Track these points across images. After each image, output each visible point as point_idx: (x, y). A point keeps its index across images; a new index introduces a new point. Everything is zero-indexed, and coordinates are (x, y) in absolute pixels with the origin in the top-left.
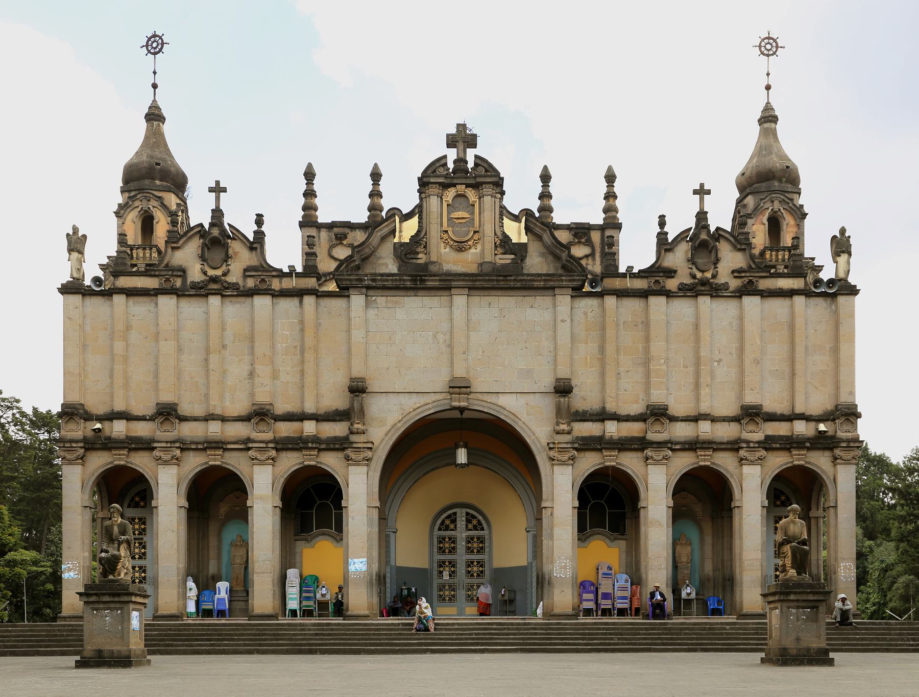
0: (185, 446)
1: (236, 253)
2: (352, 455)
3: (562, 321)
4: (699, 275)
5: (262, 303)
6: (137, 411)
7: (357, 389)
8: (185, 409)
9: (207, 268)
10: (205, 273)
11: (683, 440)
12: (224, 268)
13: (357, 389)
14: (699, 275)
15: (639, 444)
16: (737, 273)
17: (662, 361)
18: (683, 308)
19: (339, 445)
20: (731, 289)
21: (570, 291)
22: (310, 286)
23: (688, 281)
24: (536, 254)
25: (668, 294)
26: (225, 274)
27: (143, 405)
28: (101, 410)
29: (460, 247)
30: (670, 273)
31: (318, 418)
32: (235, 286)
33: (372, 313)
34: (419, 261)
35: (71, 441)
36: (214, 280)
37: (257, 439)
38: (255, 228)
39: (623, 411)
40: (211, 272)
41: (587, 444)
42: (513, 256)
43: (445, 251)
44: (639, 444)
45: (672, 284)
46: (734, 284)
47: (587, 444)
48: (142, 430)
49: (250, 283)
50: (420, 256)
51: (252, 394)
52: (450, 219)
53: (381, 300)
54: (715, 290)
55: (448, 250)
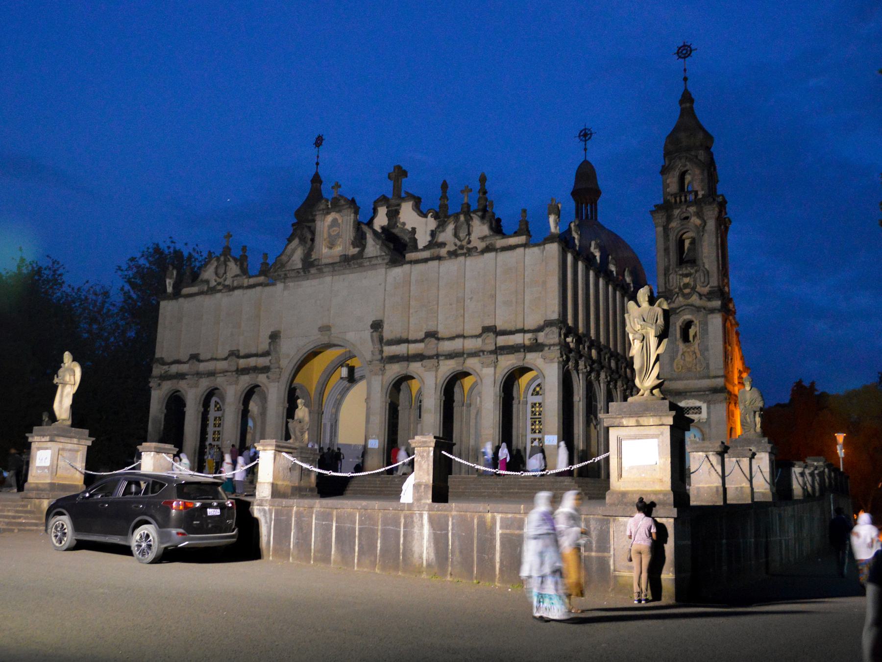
0: (199, 375)
4: (459, 243)
7: (274, 337)
9: (217, 279)
10: (216, 281)
11: (447, 353)
14: (459, 243)
15: (419, 357)
16: (483, 239)
17: (435, 303)
18: (450, 267)
19: (265, 369)
20: (479, 250)
22: (261, 281)
23: (453, 248)
25: (439, 258)
26: (225, 280)
27: (184, 355)
29: (331, 246)
30: (443, 245)
31: (256, 355)
33: (286, 293)
38: (241, 253)
40: (219, 280)
41: (394, 359)
43: (325, 250)
44: (419, 357)
45: (443, 252)
46: (481, 245)
47: (394, 359)
48: (184, 368)
52: (329, 233)
53: (291, 284)
54: (470, 252)
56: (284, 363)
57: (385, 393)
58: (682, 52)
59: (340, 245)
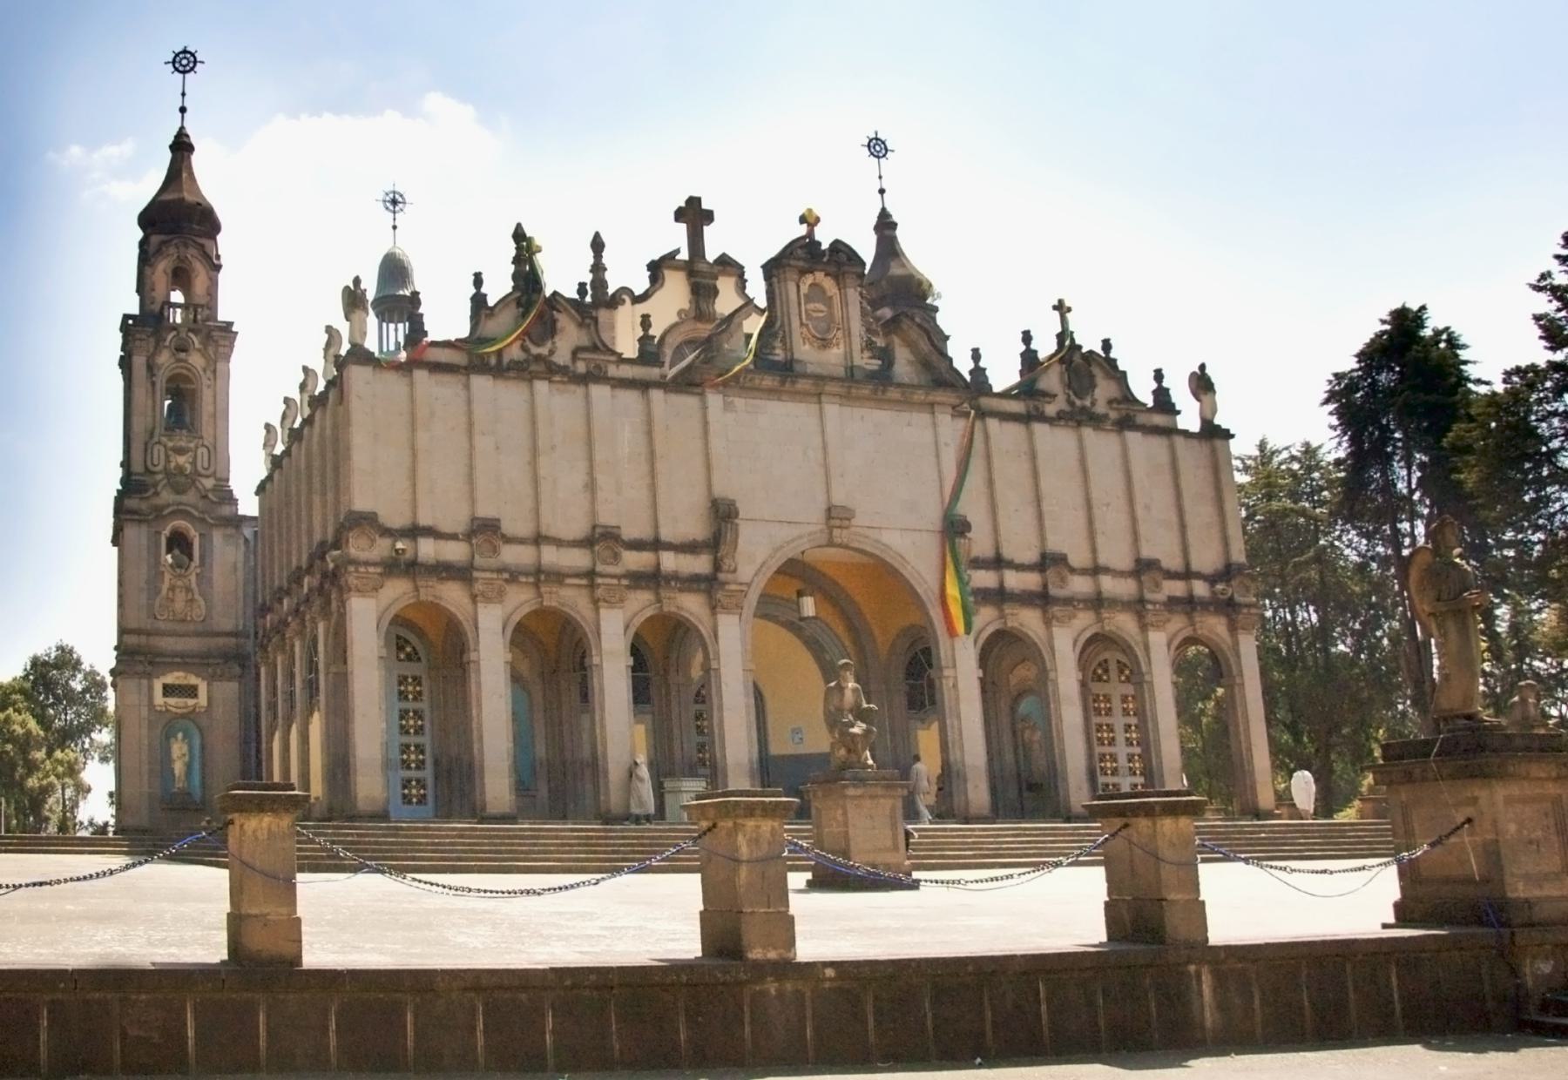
1: (563, 330)
2: (725, 601)
3: (946, 444)
5: (599, 392)
6: (446, 527)
7: (723, 514)
8: (508, 527)
12: (549, 345)
13: (723, 514)
21: (950, 410)
24: (904, 361)
28: (397, 521)
32: (563, 370)
34: (776, 358)
35: (367, 564)
36: (538, 358)
37: (604, 572)
39: (1018, 560)
40: (535, 350)
42: (880, 362)
49: (581, 367)
50: (778, 351)
51: (593, 513)
55: (807, 347)
56: (746, 571)
57: (1077, 656)
58: (189, 62)
59: (838, 345)
